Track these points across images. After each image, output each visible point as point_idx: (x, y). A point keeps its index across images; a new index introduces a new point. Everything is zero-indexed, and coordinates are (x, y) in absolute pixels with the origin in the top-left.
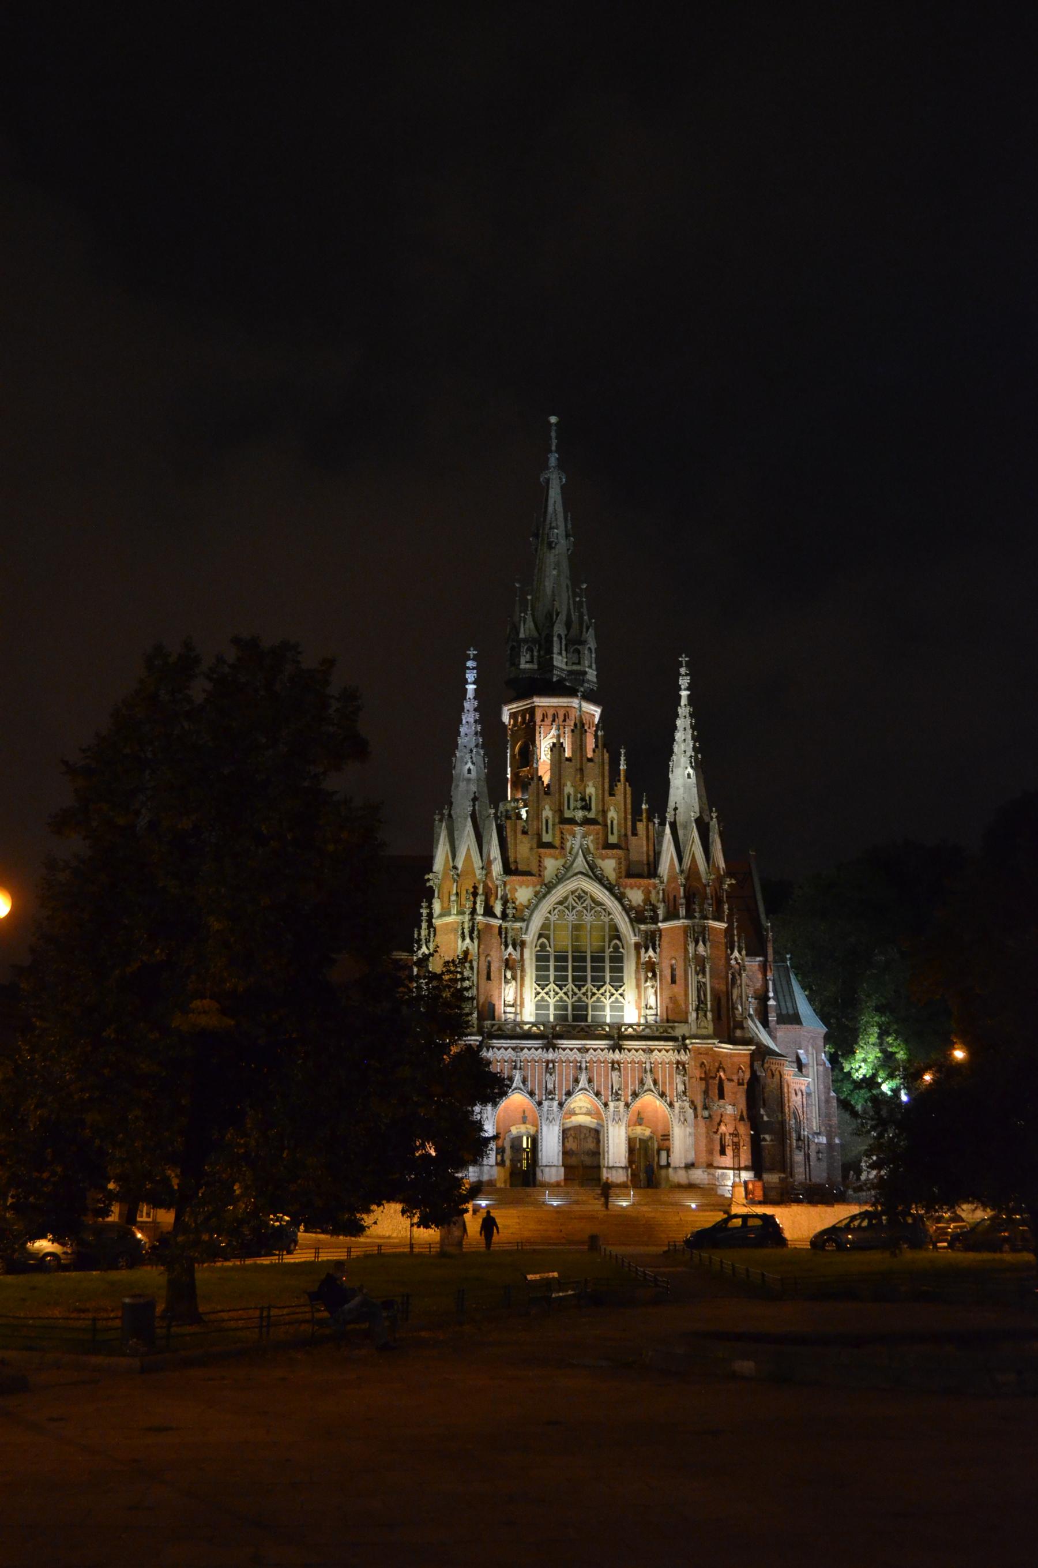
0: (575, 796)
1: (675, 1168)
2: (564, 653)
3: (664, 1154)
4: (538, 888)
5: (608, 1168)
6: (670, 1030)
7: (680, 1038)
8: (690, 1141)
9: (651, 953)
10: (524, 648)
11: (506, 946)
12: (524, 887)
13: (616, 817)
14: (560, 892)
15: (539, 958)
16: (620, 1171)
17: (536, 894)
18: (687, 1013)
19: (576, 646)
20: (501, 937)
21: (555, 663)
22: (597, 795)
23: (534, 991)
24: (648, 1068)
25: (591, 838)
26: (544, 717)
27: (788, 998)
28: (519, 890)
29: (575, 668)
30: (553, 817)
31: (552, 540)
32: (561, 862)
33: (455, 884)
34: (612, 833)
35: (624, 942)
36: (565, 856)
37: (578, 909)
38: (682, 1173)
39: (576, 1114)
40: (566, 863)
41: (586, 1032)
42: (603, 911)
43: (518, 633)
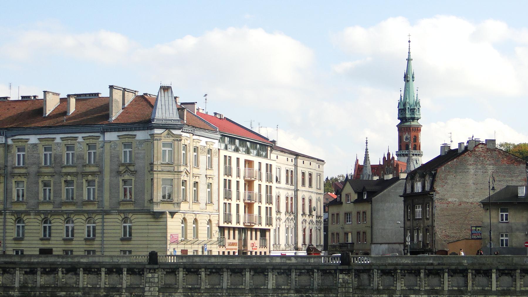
2: (410, 112)
26: (404, 129)
29: (413, 116)
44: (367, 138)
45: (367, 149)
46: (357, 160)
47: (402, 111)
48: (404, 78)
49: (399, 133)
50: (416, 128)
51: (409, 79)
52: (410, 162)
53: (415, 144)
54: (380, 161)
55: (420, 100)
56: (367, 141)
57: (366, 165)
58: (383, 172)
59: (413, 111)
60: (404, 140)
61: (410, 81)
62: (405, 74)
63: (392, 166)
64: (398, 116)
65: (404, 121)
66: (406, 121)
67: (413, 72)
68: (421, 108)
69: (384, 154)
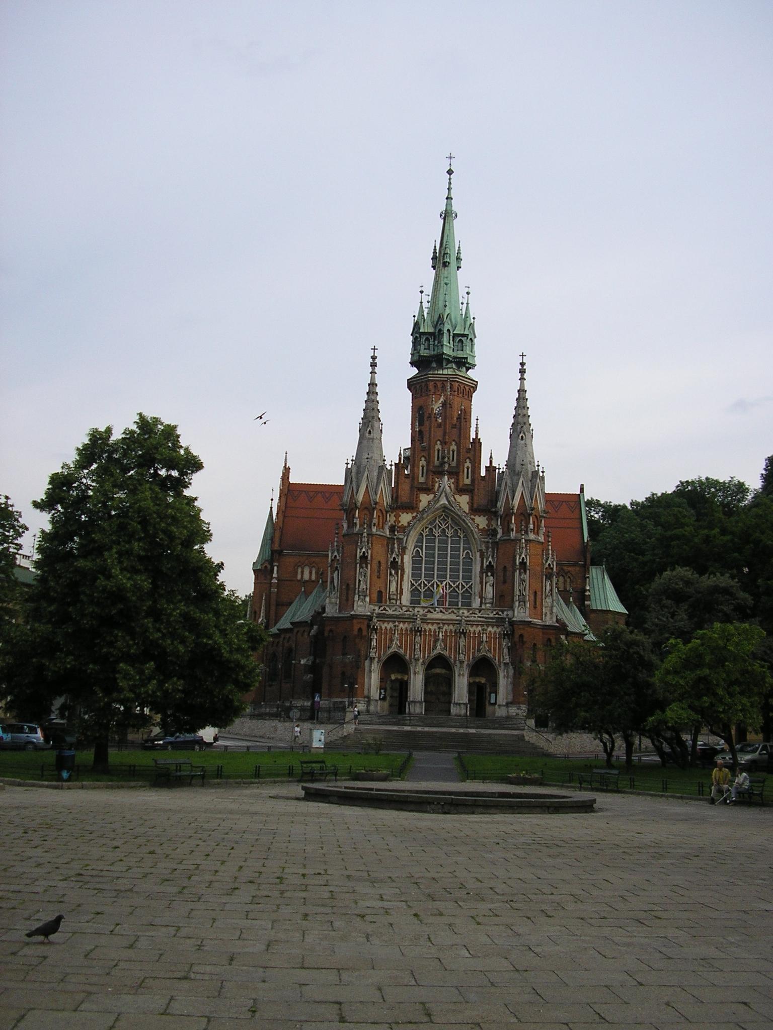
0: (443, 451)
1: (500, 706)
2: (451, 342)
3: (493, 695)
4: (414, 514)
5: (455, 703)
6: (500, 613)
7: (507, 620)
8: (510, 687)
9: (490, 559)
10: (423, 340)
11: (392, 553)
12: (405, 514)
13: (470, 466)
16: (462, 706)
17: (414, 518)
18: (513, 601)
19: (460, 338)
20: (388, 546)
23: (410, 583)
24: (485, 639)
25: (453, 480)
26: (436, 387)
27: (601, 590)
28: (402, 515)
29: (460, 354)
30: (428, 465)
31: (445, 260)
32: (432, 496)
33: (357, 511)
34: (468, 478)
35: (473, 552)
36: (434, 493)
37: (442, 527)
38: (503, 708)
39: (436, 668)
40: (435, 497)
41: (444, 613)
42: (459, 530)
43: (419, 329)
45: (372, 385)
46: (287, 470)
47: (427, 339)
48: (432, 259)
49: (414, 398)
50: (467, 388)
51: (448, 260)
52: (524, 433)
55: (474, 318)
57: (370, 431)
59: (464, 338)
61: (451, 265)
62: (435, 249)
63: (458, 445)
65: (434, 365)
66: (440, 366)
67: (459, 247)
68: (476, 340)
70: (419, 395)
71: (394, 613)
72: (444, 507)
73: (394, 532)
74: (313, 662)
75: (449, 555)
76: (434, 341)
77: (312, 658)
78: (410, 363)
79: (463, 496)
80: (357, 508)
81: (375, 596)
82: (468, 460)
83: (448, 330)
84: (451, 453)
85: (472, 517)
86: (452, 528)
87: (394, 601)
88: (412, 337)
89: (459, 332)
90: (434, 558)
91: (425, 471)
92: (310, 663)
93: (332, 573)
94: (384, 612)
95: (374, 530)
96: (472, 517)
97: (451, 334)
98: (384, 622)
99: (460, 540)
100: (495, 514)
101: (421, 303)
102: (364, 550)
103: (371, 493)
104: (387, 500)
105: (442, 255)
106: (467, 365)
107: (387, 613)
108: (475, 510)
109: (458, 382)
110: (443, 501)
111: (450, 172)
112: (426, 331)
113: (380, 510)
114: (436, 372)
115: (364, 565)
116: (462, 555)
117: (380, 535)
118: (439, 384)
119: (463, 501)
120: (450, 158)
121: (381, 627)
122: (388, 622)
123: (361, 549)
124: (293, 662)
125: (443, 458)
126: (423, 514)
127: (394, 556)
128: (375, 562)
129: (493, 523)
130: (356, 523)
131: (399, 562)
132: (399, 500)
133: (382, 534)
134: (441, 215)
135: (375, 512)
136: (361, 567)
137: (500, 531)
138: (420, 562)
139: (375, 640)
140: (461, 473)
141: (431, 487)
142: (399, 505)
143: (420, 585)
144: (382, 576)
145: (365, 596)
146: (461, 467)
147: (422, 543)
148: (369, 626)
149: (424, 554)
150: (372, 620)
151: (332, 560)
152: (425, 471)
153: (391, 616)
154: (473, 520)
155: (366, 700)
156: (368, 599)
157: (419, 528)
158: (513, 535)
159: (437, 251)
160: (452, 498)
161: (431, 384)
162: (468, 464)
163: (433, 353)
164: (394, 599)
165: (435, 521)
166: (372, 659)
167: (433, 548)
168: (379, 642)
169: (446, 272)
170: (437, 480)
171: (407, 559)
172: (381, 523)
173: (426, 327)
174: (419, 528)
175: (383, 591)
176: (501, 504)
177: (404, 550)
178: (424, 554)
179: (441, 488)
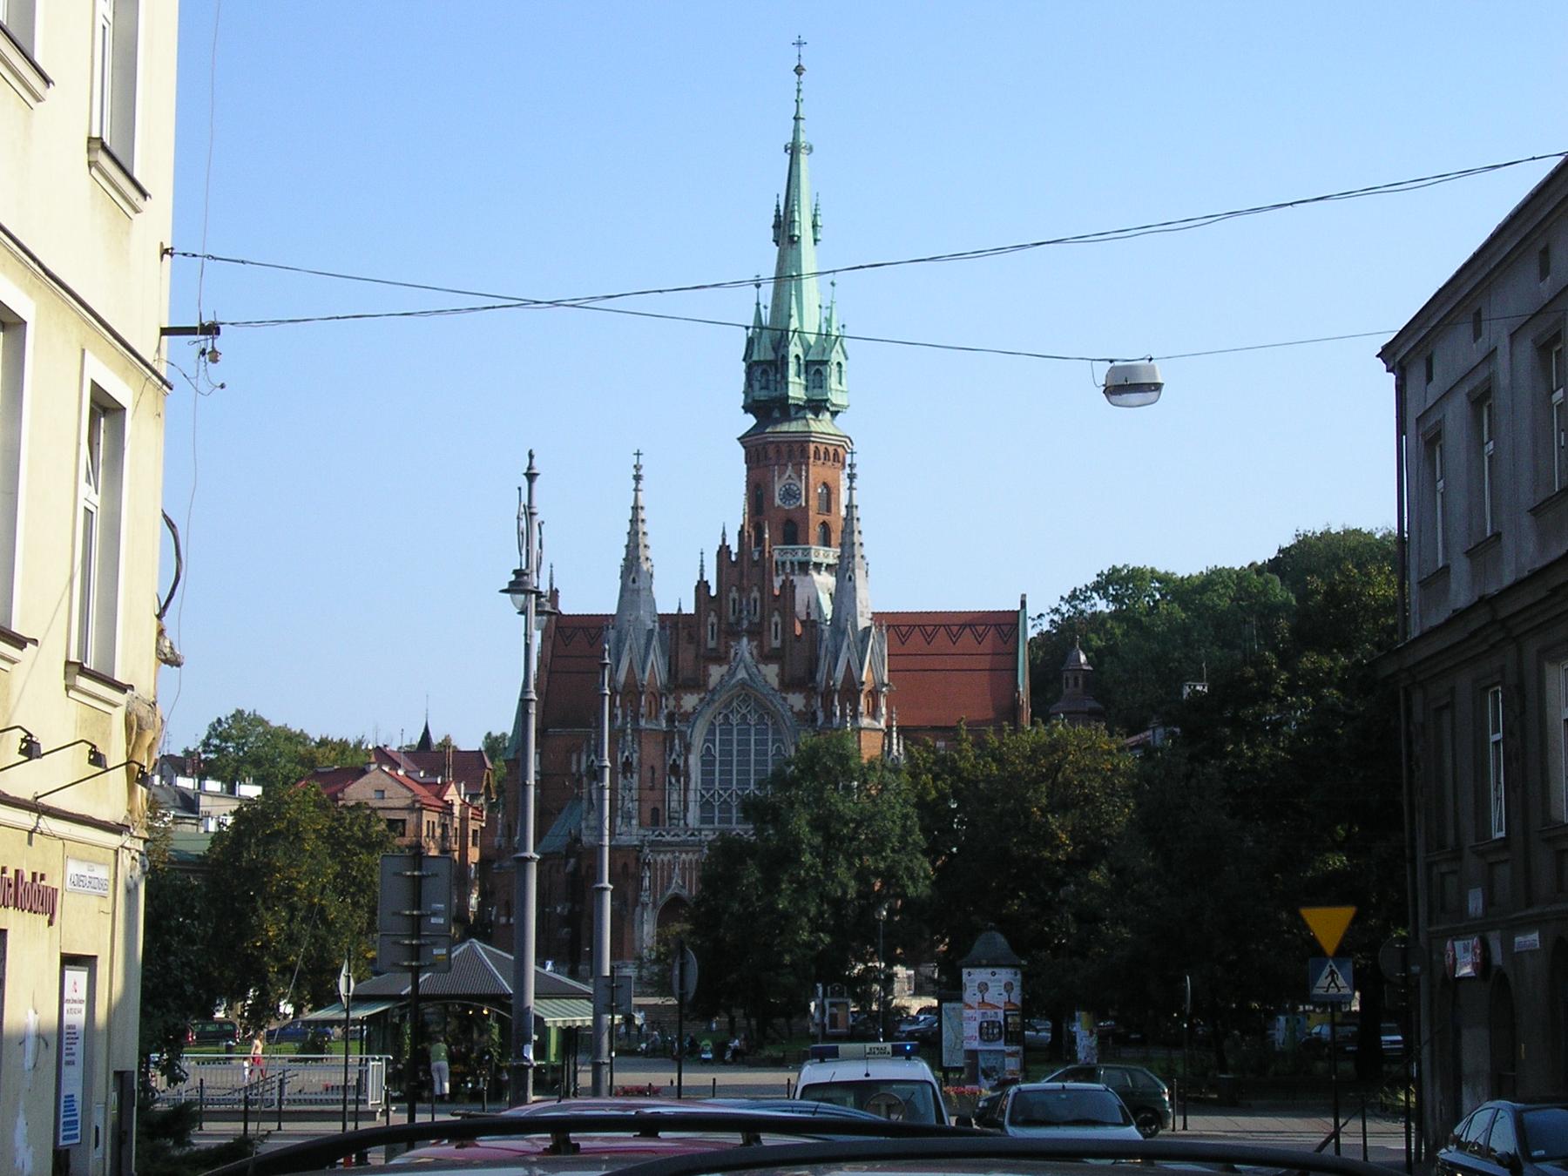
2: (802, 377)
4: (702, 695)
14: (721, 698)
15: (704, 763)
17: (701, 700)
19: (817, 367)
20: (665, 744)
21: (791, 394)
22: (762, 599)
23: (699, 794)
25: (755, 643)
26: (778, 451)
30: (720, 619)
32: (725, 668)
36: (729, 663)
40: (730, 669)
44: (638, 454)
47: (764, 372)
48: (774, 227)
49: (749, 469)
50: (831, 449)
52: (853, 571)
53: (825, 518)
54: (702, 566)
56: (637, 467)
57: (634, 581)
58: (715, 621)
60: (778, 501)
61: (803, 239)
62: (778, 210)
63: (761, 591)
64: (743, 396)
65: (776, 414)
69: (724, 534)
70: (754, 465)
71: (673, 839)
72: (743, 683)
73: (674, 722)
74: (570, 911)
75: (753, 751)
76: (775, 376)
77: (568, 905)
78: (743, 407)
79: (770, 666)
80: (617, 692)
81: (647, 816)
82: (776, 613)
83: (797, 357)
84: (752, 603)
85: (784, 695)
86: (756, 711)
87: (676, 822)
88: (744, 364)
89: (816, 358)
90: (731, 756)
91: (715, 631)
92: (566, 913)
93: (590, 784)
94: (660, 838)
95: (643, 723)
96: (784, 695)
97: (801, 362)
98: (659, 852)
99: (767, 729)
100: (814, 689)
101: (758, 304)
102: (626, 754)
103: (637, 671)
104: (662, 677)
105: (788, 222)
106: (831, 409)
107: (664, 839)
108: (788, 684)
109: (813, 442)
110: (742, 674)
111: (799, 70)
112: (762, 359)
113: (652, 693)
114: (778, 430)
115: (629, 775)
116: (771, 749)
117: (651, 730)
118: (784, 448)
119: (771, 672)
120: (799, 44)
121: (655, 861)
122: (665, 852)
123: (623, 752)
124: (547, 910)
125: (741, 611)
126: (714, 695)
127: (674, 756)
128: (646, 768)
129: (813, 702)
130: (616, 715)
131: (682, 765)
132: (680, 677)
133: (654, 727)
134: (786, 151)
135: (643, 698)
136: (625, 778)
137: (820, 715)
138: (713, 763)
139: (647, 880)
140: (765, 633)
141: (723, 656)
142: (678, 682)
143: (713, 796)
144: (657, 786)
145: (631, 818)
146: (766, 623)
147: (715, 735)
148: (638, 859)
149: (717, 750)
150: (641, 851)
151: (588, 766)
152: (715, 631)
153: (669, 844)
154: (785, 699)
155: (638, 962)
156: (634, 822)
157: (708, 714)
158: (837, 721)
159: (782, 213)
160: (755, 670)
161: (772, 453)
162: (776, 618)
163: (774, 394)
164: (675, 818)
165: (731, 703)
166: (645, 905)
167: (730, 742)
168: (653, 880)
169: (794, 251)
170: (732, 643)
171: (694, 760)
172: (653, 712)
173: (762, 354)
174: (708, 714)
175: (659, 806)
176: (821, 676)
177: (687, 748)
178: (717, 750)
179: (739, 656)
